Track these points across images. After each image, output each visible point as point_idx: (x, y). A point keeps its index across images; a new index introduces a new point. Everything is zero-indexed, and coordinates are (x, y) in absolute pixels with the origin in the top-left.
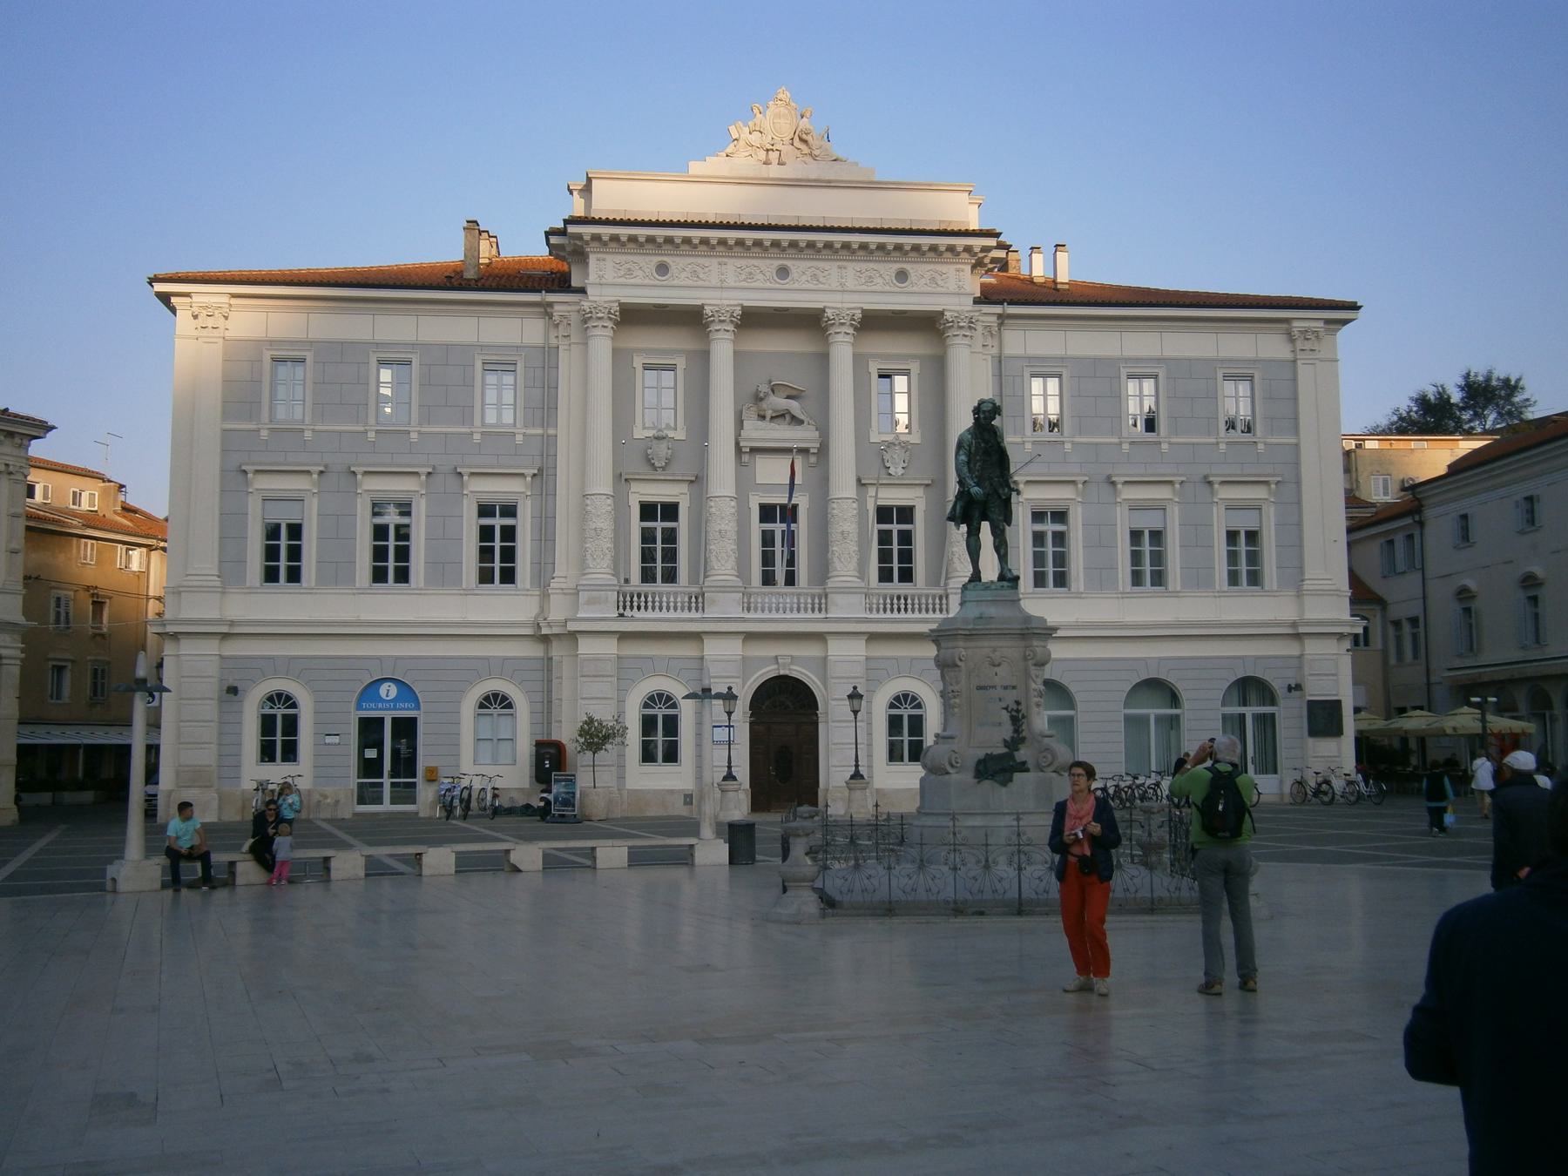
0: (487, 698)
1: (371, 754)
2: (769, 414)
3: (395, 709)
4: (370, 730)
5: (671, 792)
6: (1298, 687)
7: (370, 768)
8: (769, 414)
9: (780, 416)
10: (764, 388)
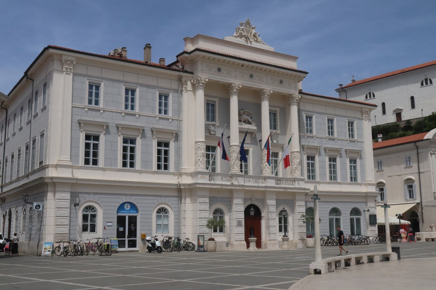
0: (159, 209)
1: (121, 229)
2: (243, 120)
3: (129, 213)
4: (121, 221)
5: (222, 242)
6: (368, 211)
7: (120, 234)
8: (243, 120)
9: (245, 122)
10: (242, 112)
